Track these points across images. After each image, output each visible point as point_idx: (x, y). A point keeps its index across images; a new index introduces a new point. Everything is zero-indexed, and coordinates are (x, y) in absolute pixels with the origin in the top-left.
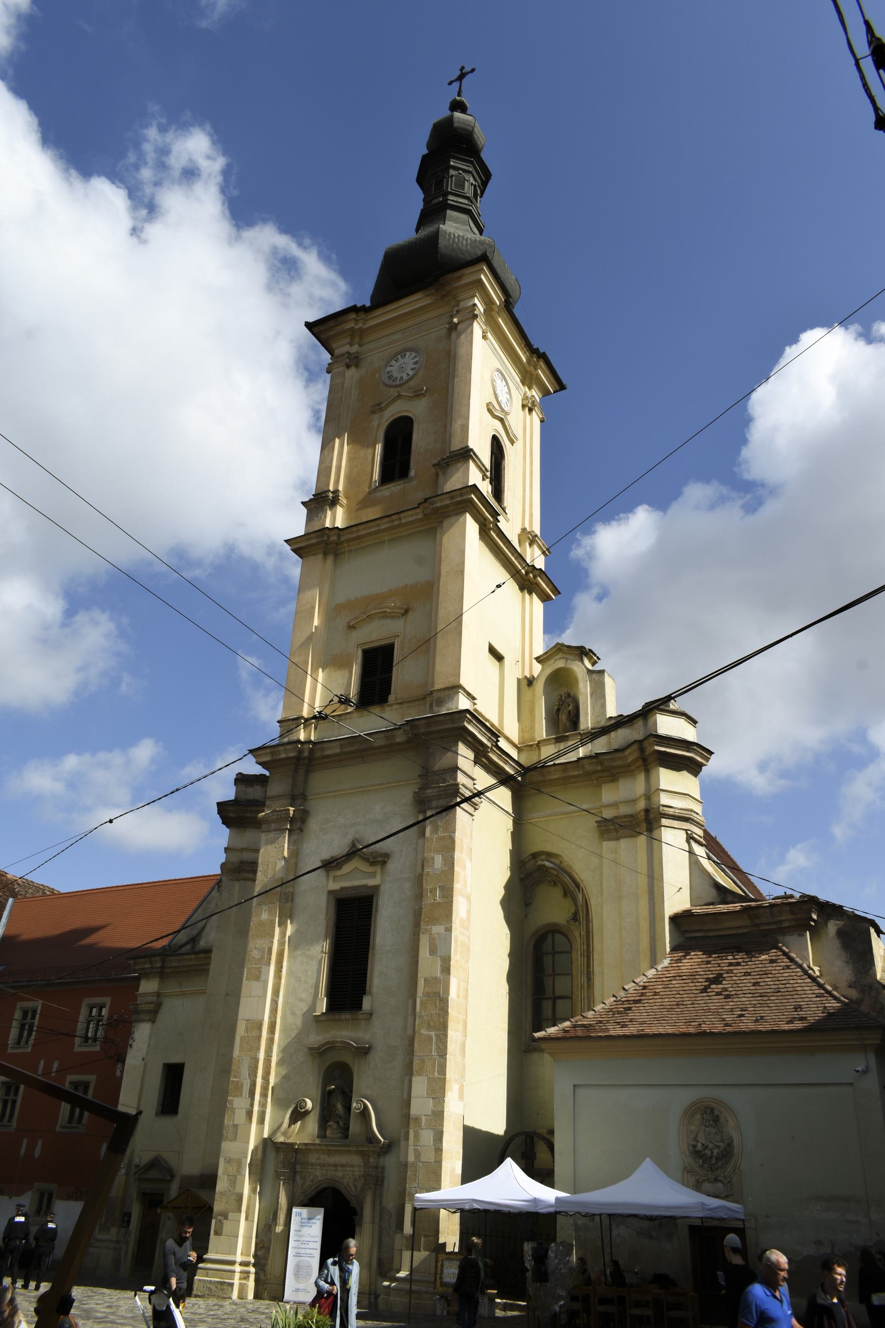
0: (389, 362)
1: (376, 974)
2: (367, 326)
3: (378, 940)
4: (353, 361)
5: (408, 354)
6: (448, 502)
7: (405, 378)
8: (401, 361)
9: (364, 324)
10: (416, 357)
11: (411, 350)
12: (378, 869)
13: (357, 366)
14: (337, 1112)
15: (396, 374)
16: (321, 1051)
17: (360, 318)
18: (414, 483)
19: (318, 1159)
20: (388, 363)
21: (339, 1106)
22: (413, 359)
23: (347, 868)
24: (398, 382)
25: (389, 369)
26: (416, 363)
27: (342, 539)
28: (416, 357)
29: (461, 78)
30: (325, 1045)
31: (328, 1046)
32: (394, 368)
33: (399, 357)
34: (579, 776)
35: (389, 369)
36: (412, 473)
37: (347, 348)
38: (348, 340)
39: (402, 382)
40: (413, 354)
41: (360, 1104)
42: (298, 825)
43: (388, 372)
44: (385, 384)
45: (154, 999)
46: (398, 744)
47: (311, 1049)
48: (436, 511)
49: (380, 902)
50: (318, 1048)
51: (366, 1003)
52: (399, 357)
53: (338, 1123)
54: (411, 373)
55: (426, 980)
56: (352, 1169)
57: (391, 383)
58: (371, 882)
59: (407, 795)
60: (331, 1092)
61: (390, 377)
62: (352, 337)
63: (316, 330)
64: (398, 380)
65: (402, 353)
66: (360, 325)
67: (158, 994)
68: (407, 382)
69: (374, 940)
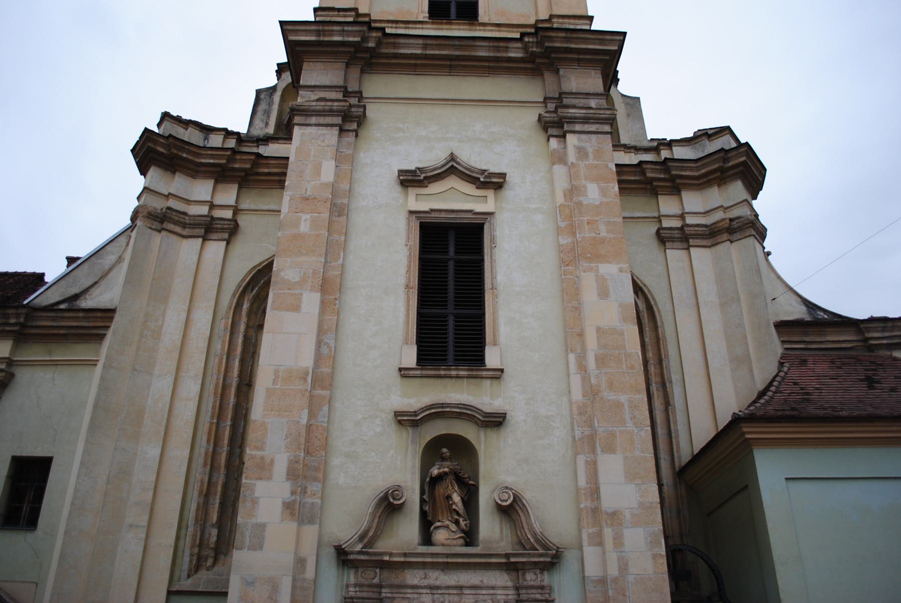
1: (502, 321)
3: (500, 278)
12: (490, 193)
14: (454, 507)
16: (418, 418)
19: (425, 578)
21: (456, 498)
23: (435, 188)
30: (427, 410)
31: (433, 411)
34: (634, 182)
41: (505, 492)
42: (354, 126)
46: (510, 60)
47: (397, 414)
49: (498, 233)
50: (415, 414)
51: (492, 358)
53: (457, 523)
55: (599, 329)
56: (491, 592)
58: (479, 207)
59: (531, 116)
60: (435, 481)
69: (493, 277)
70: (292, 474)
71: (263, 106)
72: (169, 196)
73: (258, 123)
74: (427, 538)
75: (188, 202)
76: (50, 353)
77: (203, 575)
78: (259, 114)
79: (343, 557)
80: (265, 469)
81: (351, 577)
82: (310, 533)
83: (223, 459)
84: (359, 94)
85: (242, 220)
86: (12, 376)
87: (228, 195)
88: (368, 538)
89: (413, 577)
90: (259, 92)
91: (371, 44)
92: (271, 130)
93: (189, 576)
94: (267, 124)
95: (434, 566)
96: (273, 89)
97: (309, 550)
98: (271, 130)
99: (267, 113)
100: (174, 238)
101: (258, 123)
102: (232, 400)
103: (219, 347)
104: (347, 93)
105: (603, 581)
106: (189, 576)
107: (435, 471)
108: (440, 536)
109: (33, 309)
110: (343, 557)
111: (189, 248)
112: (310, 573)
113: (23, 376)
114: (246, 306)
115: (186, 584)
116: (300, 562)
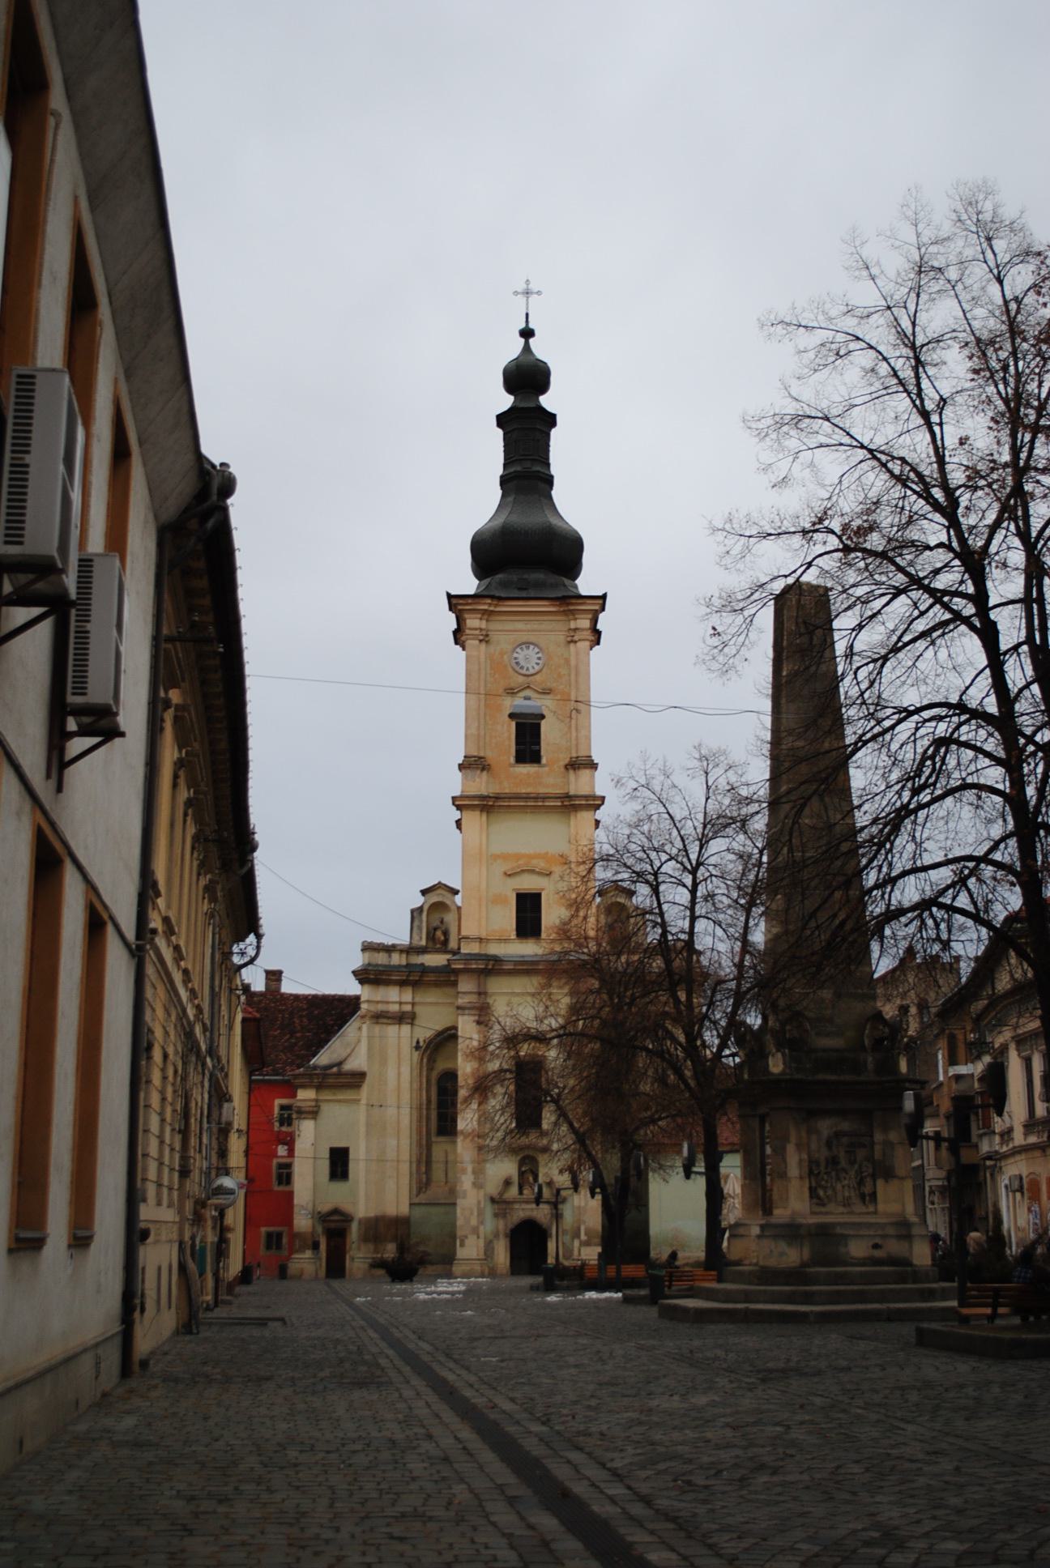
5: (532, 647)
6: (584, 802)
7: (532, 671)
8: (526, 652)
11: (535, 645)
13: (487, 642)
15: (522, 663)
18: (546, 769)
20: (514, 650)
25: (515, 655)
26: (539, 658)
29: (527, 293)
32: (521, 655)
35: (515, 655)
36: (544, 761)
38: (479, 616)
39: (527, 673)
40: (537, 650)
44: (514, 670)
45: (313, 1104)
52: (524, 646)
54: (537, 668)
57: (517, 669)
61: (517, 663)
62: (483, 614)
63: (454, 601)
65: (528, 644)
66: (492, 608)
67: (317, 1101)
68: (532, 675)
70: (474, 1172)
71: (416, 923)
72: (378, 1002)
73: (416, 937)
74: (521, 1193)
75: (388, 1003)
76: (334, 1094)
77: (422, 1195)
78: (415, 929)
79: (493, 1200)
80: (464, 1171)
81: (496, 1206)
82: (482, 1193)
83: (424, 1142)
84: (485, 993)
85: (418, 1009)
86: (319, 1107)
87: (407, 995)
88: (501, 1194)
89: (516, 1206)
90: (413, 911)
91: (490, 967)
92: (423, 943)
93: (417, 1196)
94: (421, 938)
95: (523, 1202)
96: (421, 909)
97: (482, 1198)
98: (423, 943)
99: (420, 928)
100: (384, 1026)
101: (416, 937)
102: (425, 1112)
103: (415, 1086)
104: (480, 994)
105: (579, 1207)
106: (417, 1196)
107: (523, 1169)
108: (525, 1192)
109: (315, 1067)
110: (493, 1200)
111: (392, 1030)
112: (482, 1206)
113: (327, 1110)
114: (425, 1060)
115: (416, 1201)
116: (479, 1202)
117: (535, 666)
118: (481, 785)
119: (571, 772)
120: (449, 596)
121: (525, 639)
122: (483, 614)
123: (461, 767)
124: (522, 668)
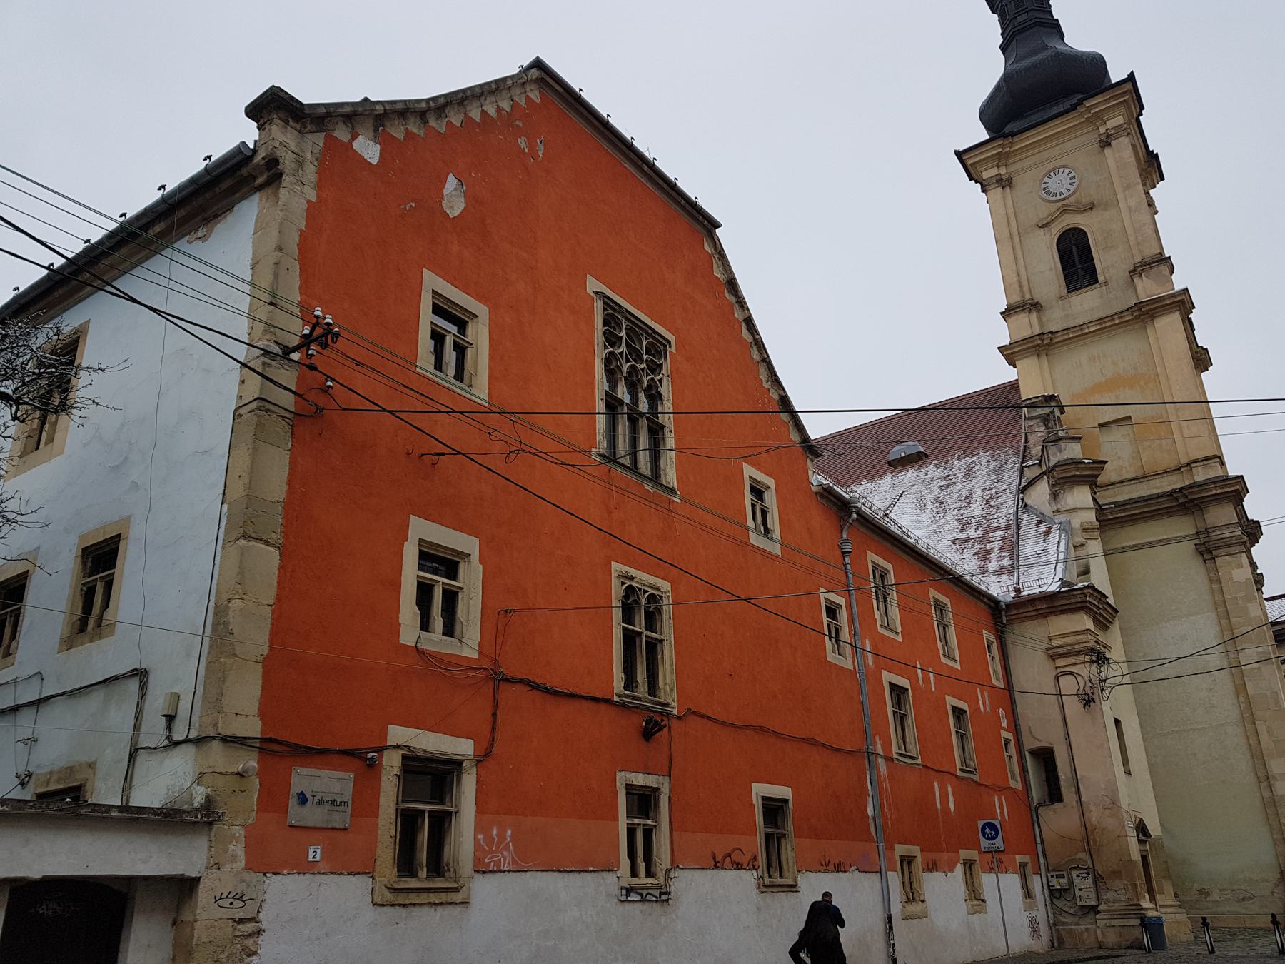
0: (1043, 178)
2: (1013, 149)
4: (1005, 183)
5: (1061, 170)
7: (1066, 194)
9: (1010, 148)
10: (1070, 172)
11: (1064, 167)
17: (1005, 143)
22: (1068, 175)
24: (1058, 197)
25: (1044, 186)
26: (1074, 177)
27: (1055, 341)
28: (1070, 172)
33: (1052, 174)
37: (994, 172)
39: (1063, 197)
40: (1067, 171)
43: (1044, 189)
48: (1147, 312)
54: (1072, 188)
62: (999, 160)
64: (1058, 194)
68: (1070, 196)
117: (1069, 187)
118: (1028, 325)
119: (1137, 280)
120: (959, 154)
121: (1051, 166)
122: (999, 160)
123: (1005, 315)
124: (1055, 195)
